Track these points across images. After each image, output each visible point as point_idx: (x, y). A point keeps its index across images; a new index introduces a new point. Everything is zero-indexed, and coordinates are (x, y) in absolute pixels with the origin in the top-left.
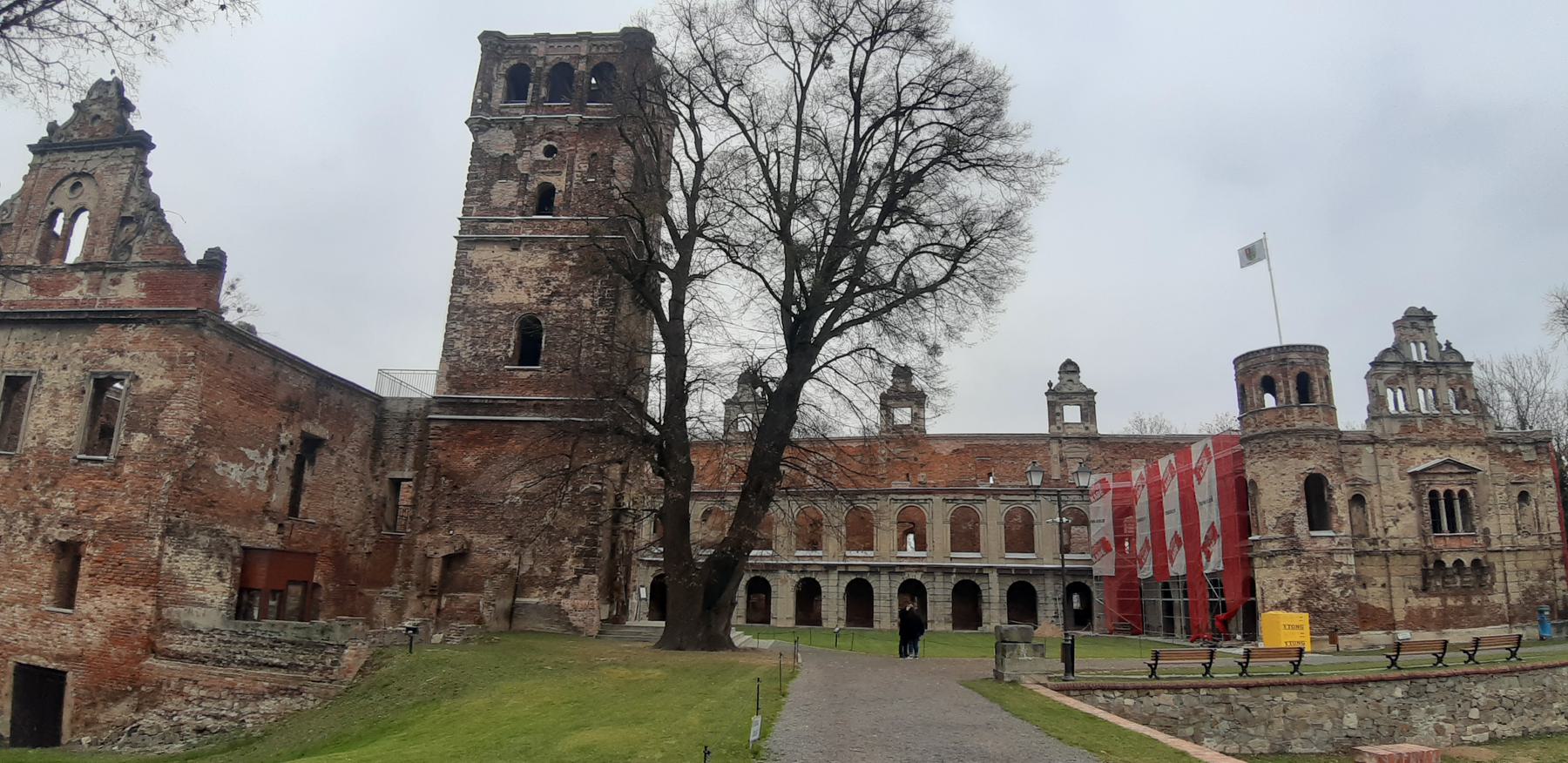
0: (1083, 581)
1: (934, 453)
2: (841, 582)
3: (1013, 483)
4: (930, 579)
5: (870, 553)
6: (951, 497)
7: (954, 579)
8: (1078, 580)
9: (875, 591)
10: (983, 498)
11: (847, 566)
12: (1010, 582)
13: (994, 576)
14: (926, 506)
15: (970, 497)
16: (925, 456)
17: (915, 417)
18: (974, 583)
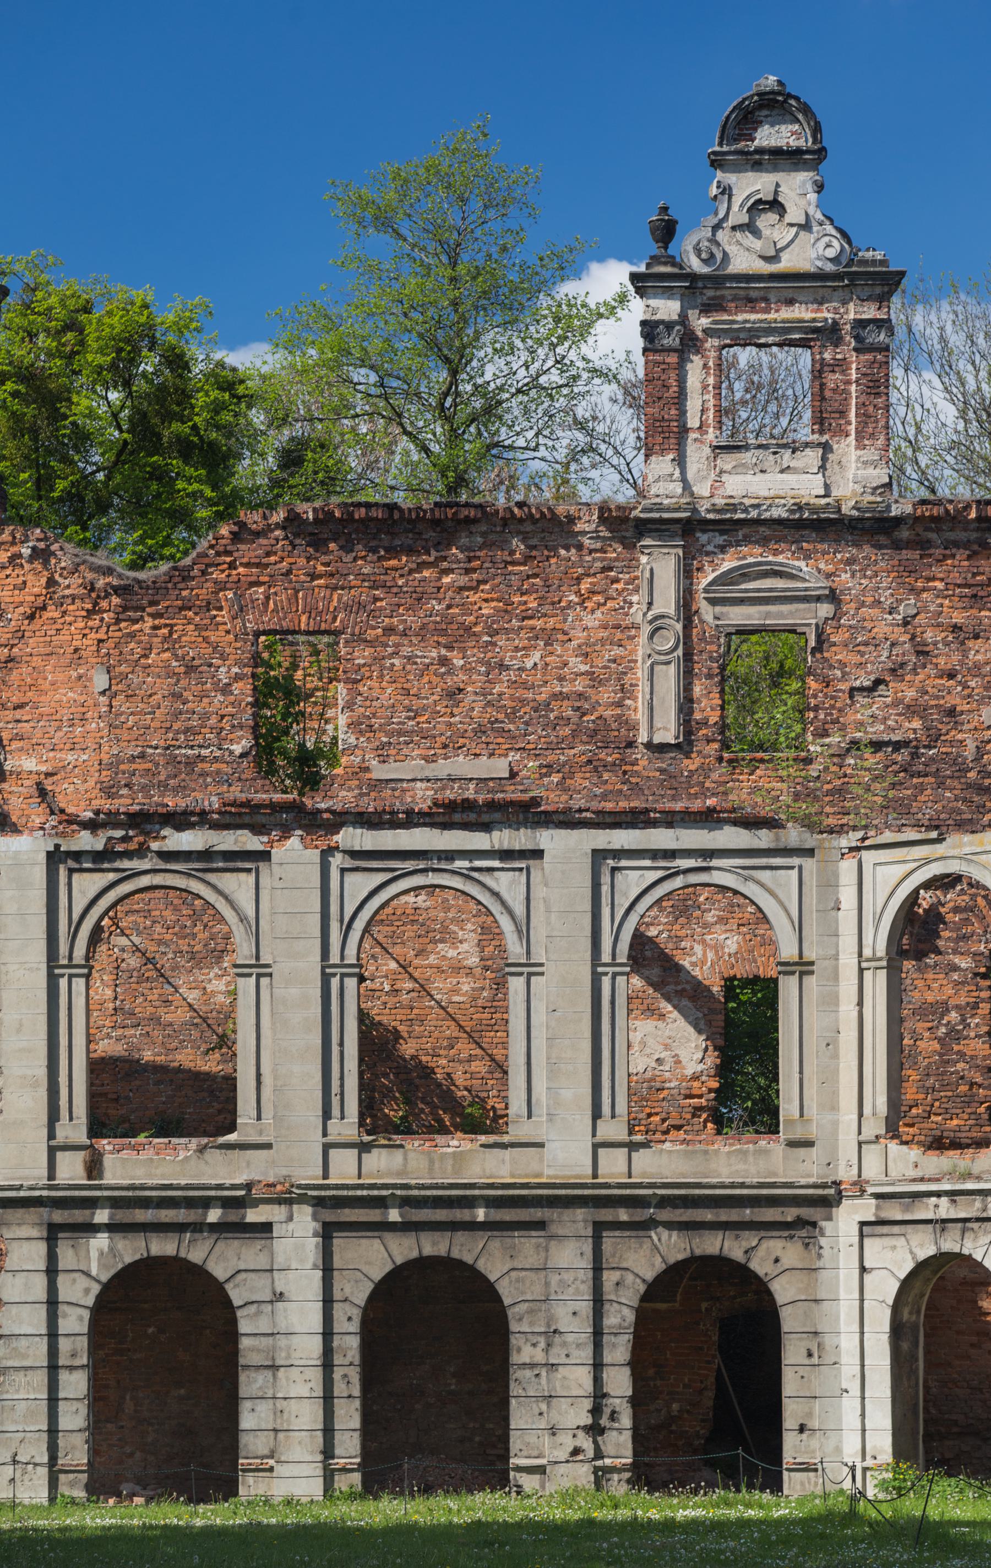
0: (734, 1248)
3: (443, 768)
8: (711, 1244)
10: (253, 843)
18: (199, 1273)
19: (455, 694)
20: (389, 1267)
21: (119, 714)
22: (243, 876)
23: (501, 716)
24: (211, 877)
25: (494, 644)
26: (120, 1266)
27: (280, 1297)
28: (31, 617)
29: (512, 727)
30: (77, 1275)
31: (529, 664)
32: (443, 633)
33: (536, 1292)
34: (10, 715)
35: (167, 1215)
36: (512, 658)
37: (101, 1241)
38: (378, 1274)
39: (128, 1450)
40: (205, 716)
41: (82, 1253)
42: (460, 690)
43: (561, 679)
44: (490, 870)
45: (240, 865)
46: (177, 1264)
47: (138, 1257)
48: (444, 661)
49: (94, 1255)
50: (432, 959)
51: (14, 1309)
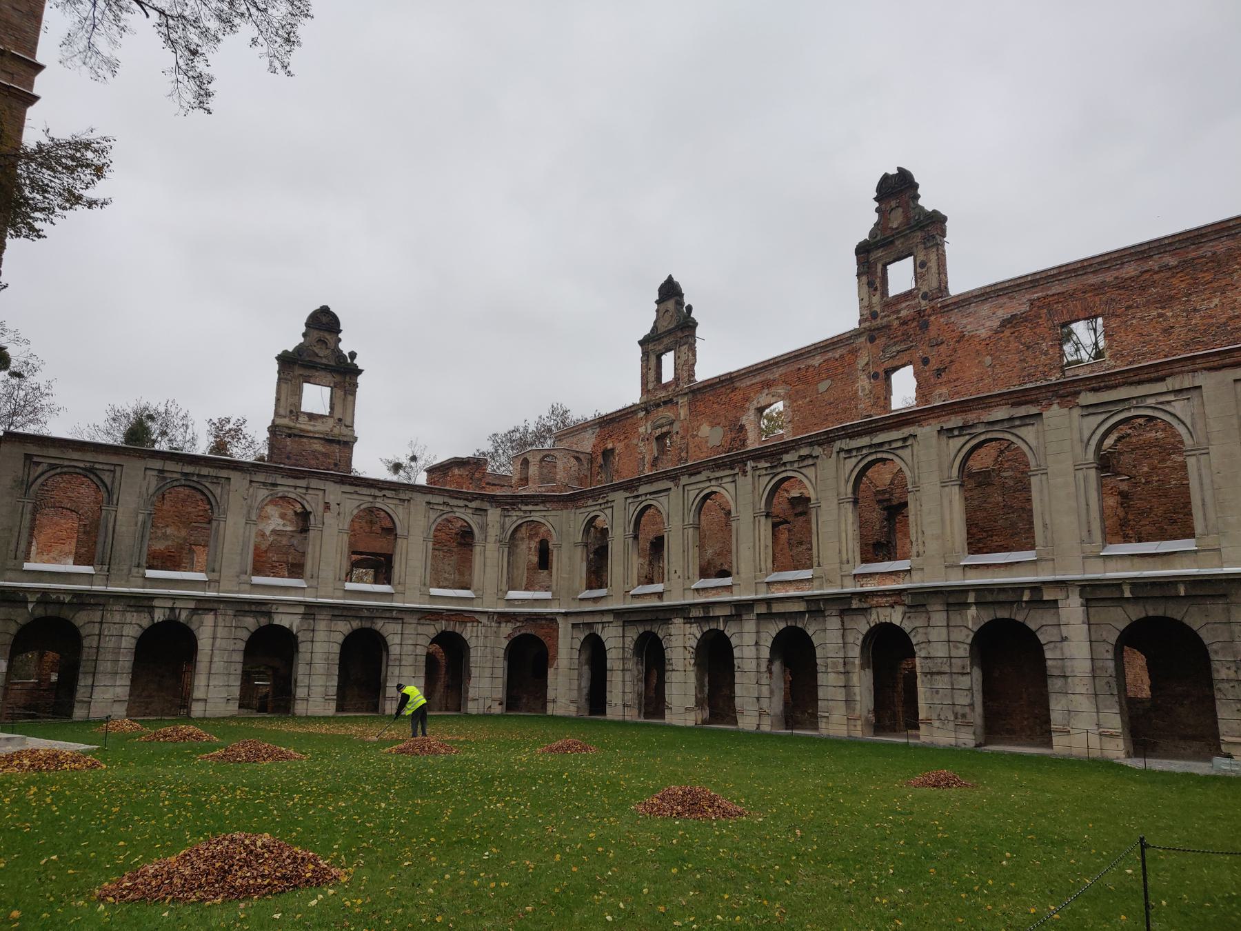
1: (962, 337)
2: (763, 635)
4: (919, 622)
5: (806, 574)
6: (955, 421)
7: (973, 618)
9: (819, 653)
10: (1034, 410)
11: (768, 602)
12: (1119, 619)
13: (1072, 608)
14: (906, 453)
15: (1000, 413)
16: (943, 348)
17: (921, 269)
18: (1022, 627)
19: (1168, 331)
20: (1127, 623)
21: (996, 375)
22: (1030, 428)
23: (1198, 335)
24: (1013, 431)
25: (1190, 301)
26: (983, 623)
27: (1064, 639)
28: (958, 342)
29: (1204, 339)
30: (962, 628)
31: (1212, 306)
32: (1159, 302)
33: (1226, 637)
34: (952, 384)
35: (1002, 597)
36: (1201, 305)
37: (972, 611)
38: (1122, 627)
39: (1026, 716)
40: (1037, 367)
41: (964, 617)
42: (1172, 327)
43: (1232, 309)
44: (1168, 402)
45: (1028, 421)
46: (1011, 622)
47: (991, 619)
48: (1160, 315)
49: (970, 618)
50: (1169, 463)
51: (934, 644)
